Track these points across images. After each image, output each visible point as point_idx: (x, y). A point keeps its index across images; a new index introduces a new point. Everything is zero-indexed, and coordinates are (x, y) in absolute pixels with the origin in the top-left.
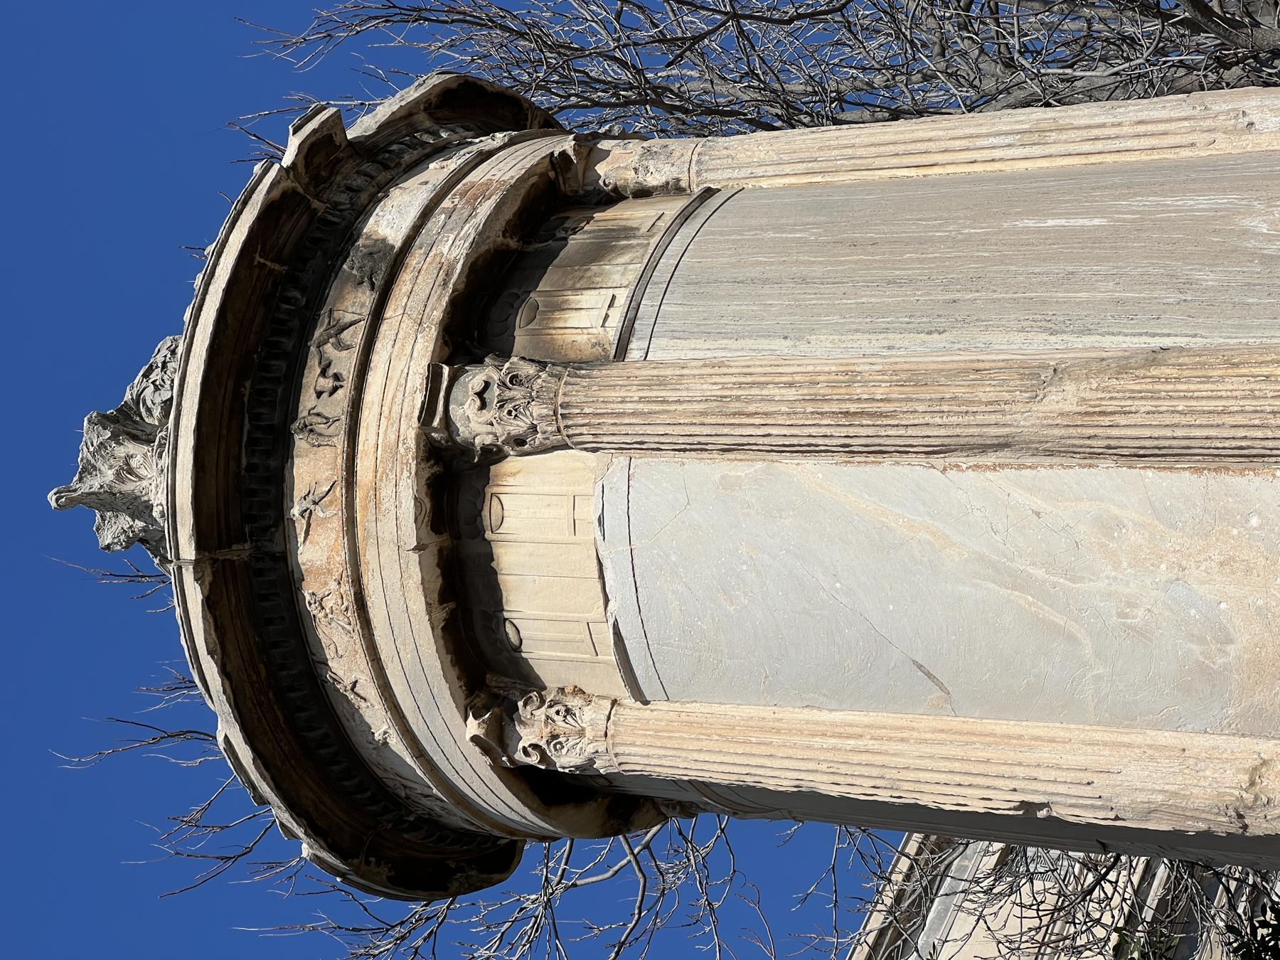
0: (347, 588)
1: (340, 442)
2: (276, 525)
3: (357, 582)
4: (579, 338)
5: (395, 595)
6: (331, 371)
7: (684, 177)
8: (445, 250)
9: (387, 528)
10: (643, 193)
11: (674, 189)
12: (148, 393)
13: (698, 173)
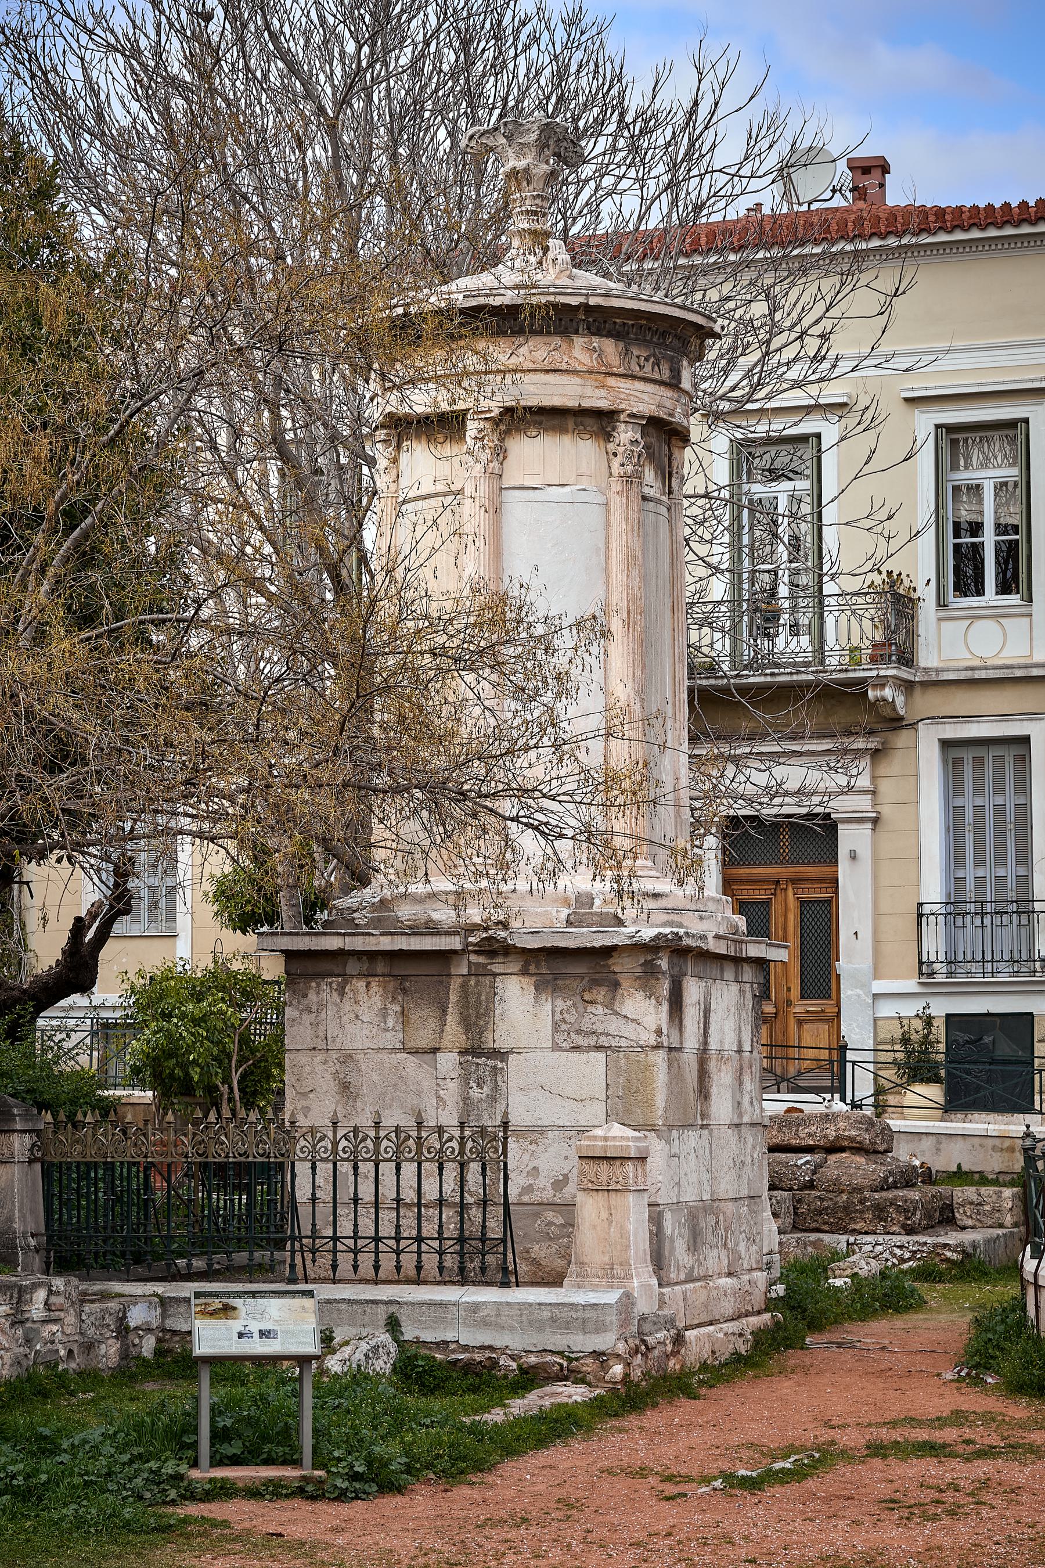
0: (564, 366)
1: (621, 371)
5: (560, 390)
9: (589, 391)
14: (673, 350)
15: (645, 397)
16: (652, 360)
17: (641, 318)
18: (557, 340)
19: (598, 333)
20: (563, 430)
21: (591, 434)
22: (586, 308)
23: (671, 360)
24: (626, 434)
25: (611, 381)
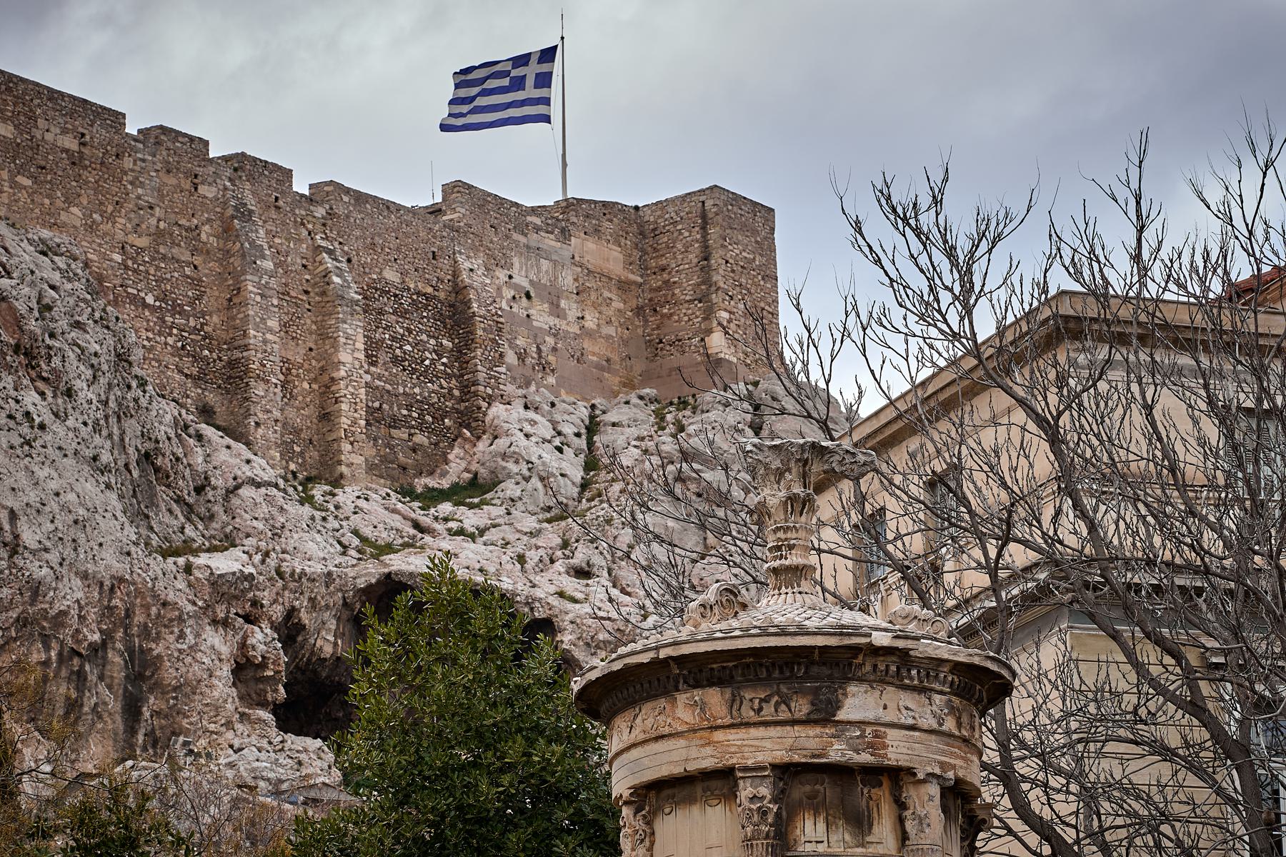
0: (667, 730)
1: (728, 721)
2: (689, 686)
3: (670, 735)
4: (798, 831)
5: (666, 758)
6: (764, 705)
7: (910, 843)
8: (836, 747)
9: (694, 753)
10: (901, 821)
11: (904, 837)
12: (837, 458)
13: (912, 850)
14: (816, 679)
15: (768, 744)
16: (776, 698)
17: (744, 656)
18: (662, 702)
19: (697, 685)
20: (690, 800)
21: (719, 798)
22: (681, 660)
23: (816, 691)
24: (746, 791)
25: (719, 736)
